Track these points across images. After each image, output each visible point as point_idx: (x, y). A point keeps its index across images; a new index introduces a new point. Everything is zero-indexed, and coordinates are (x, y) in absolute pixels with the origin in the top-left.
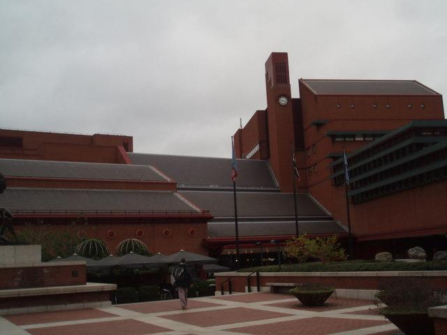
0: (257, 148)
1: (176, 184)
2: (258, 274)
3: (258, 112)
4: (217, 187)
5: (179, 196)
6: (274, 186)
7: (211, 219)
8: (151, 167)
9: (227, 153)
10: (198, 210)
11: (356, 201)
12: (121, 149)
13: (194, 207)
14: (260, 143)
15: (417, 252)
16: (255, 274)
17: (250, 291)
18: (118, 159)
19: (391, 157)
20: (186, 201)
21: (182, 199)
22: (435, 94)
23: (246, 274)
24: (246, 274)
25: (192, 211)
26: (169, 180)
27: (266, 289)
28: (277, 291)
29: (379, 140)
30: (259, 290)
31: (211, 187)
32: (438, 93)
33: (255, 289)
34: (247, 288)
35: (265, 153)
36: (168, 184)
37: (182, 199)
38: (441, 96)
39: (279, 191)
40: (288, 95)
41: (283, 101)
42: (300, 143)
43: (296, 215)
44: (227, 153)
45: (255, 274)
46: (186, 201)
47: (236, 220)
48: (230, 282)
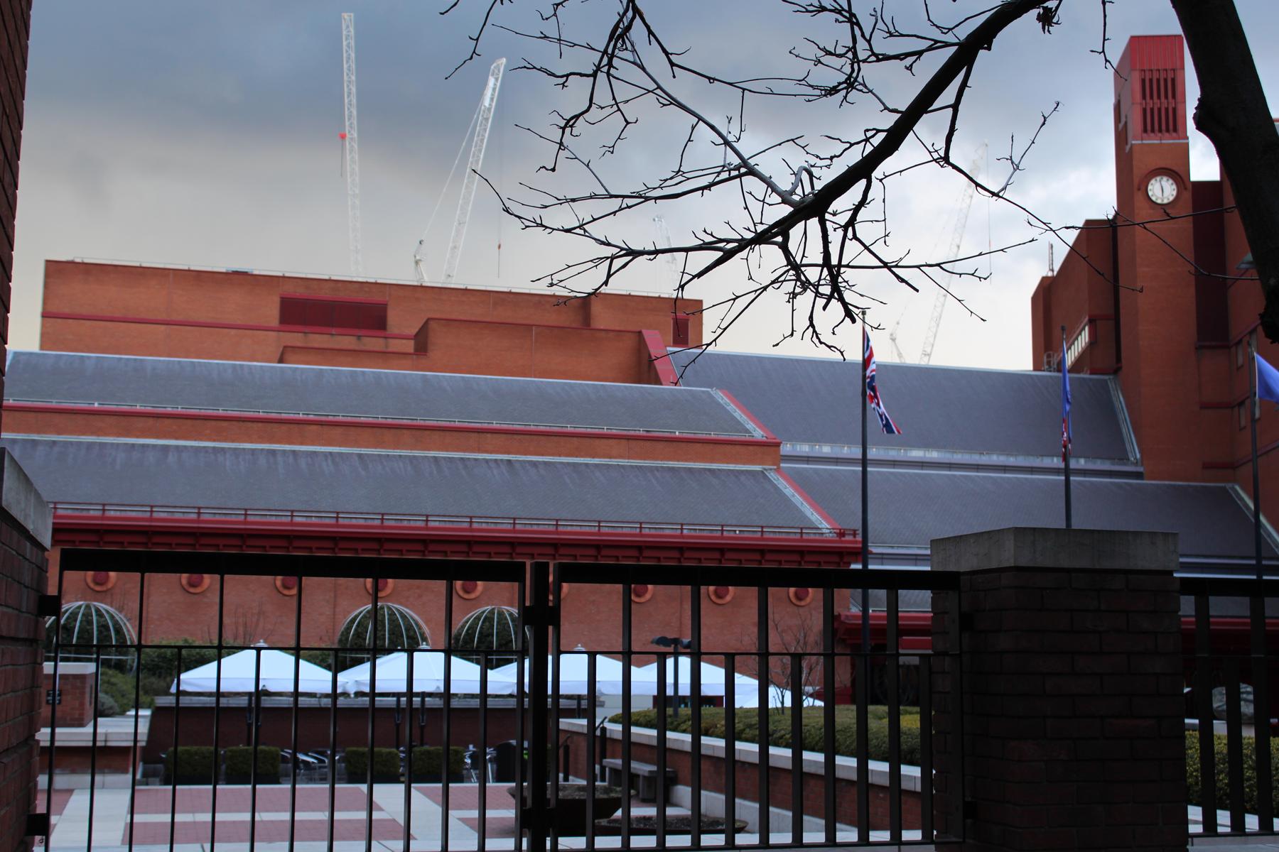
0: (1083, 339)
1: (778, 445)
3: (1091, 228)
4: (934, 455)
6: (1124, 458)
8: (720, 397)
10: (824, 525)
12: (659, 342)
13: (815, 517)
14: (1092, 322)
18: (644, 368)
21: (789, 491)
26: (758, 434)
31: (916, 454)
35: (1108, 356)
37: (789, 491)
39: (1138, 475)
40: (1179, 174)
41: (1162, 190)
46: (797, 499)
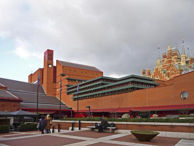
2: (80, 122)
4: (23, 91)
5: (8, 92)
7: (21, 101)
9: (26, 80)
15: (155, 116)
16: (78, 122)
17: (72, 130)
19: (86, 88)
20: (11, 94)
23: (72, 122)
24: (72, 122)
25: (14, 98)
27: (83, 129)
29: (83, 83)
30: (80, 129)
31: (20, 91)
33: (77, 129)
36: (4, 87)
37: (10, 93)
42: (55, 81)
43: (60, 103)
44: (26, 80)
45: (78, 122)
47: (38, 103)
48: (59, 125)
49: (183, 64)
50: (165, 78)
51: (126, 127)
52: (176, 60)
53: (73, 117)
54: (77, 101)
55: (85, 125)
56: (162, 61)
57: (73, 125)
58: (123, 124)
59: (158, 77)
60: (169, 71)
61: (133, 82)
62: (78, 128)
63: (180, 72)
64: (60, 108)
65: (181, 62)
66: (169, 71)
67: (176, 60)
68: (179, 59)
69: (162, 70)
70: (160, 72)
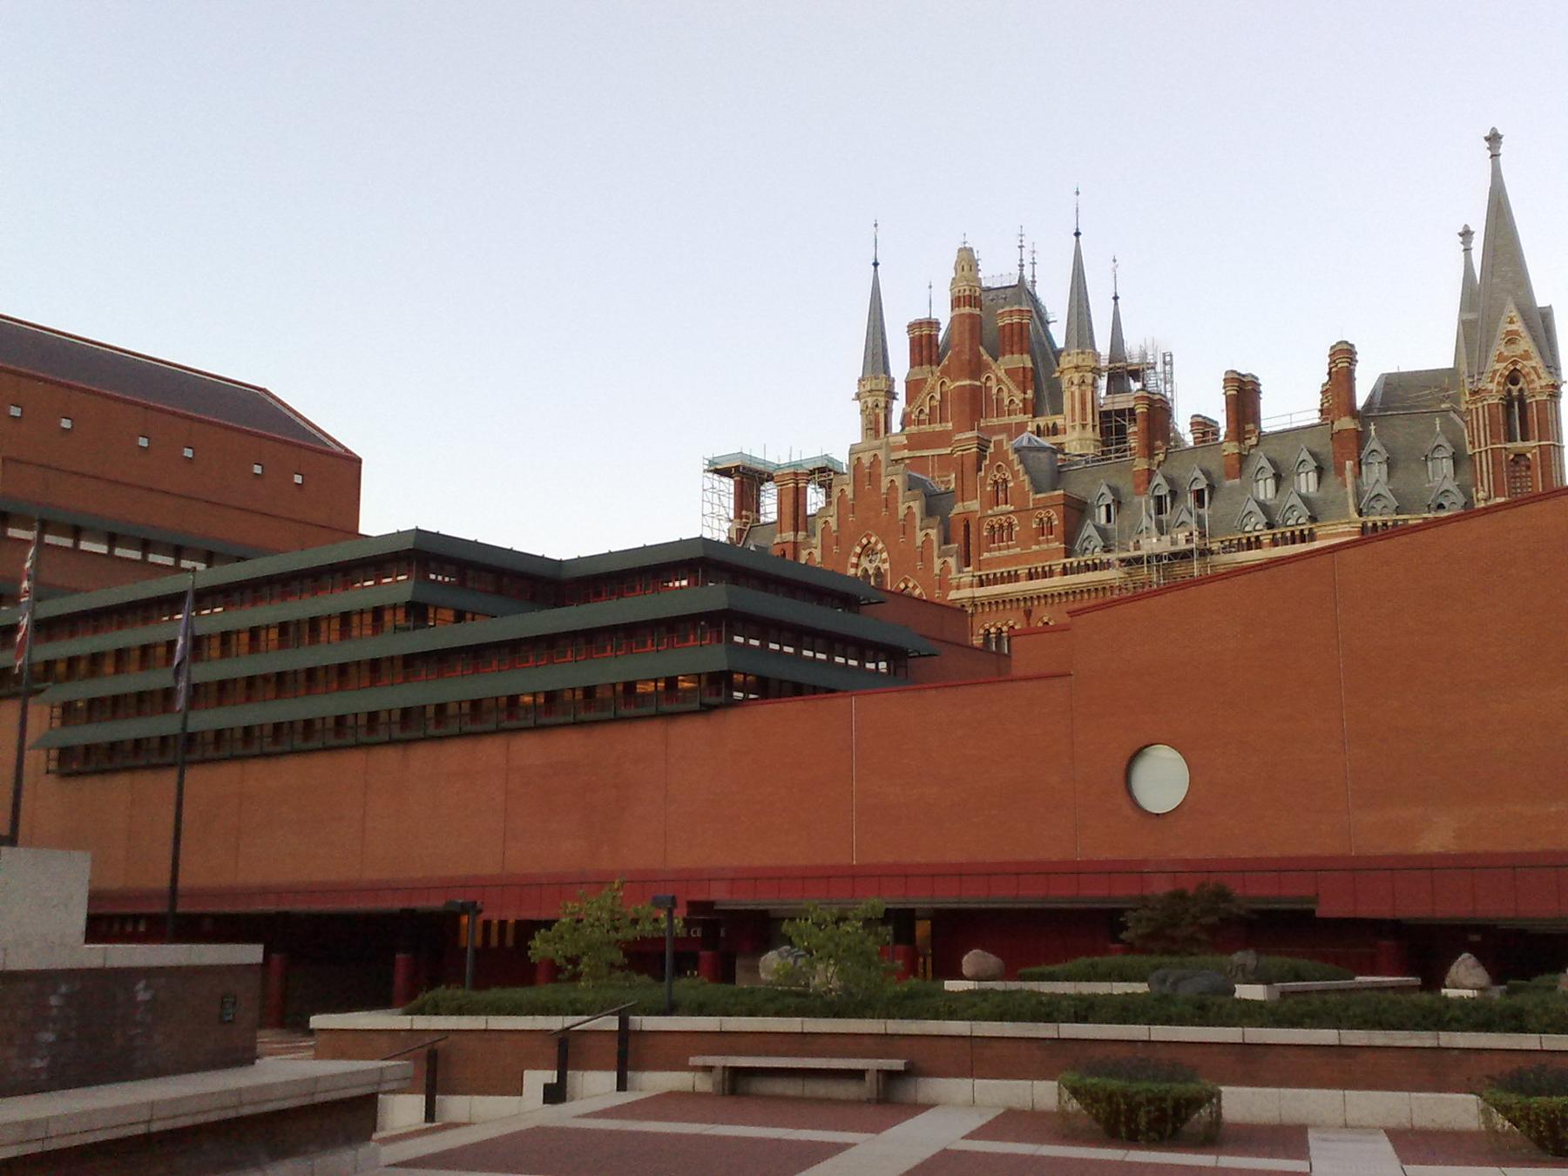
2: (624, 1023)
11: (76, 763)
17: (555, 1094)
22: (338, 449)
23: (556, 1023)
24: (556, 1023)
28: (737, 1082)
30: (622, 1085)
32: (347, 450)
34: (537, 1079)
38: (359, 461)
49: (1078, 440)
50: (937, 564)
51: (976, 1060)
52: (1018, 397)
53: (479, 984)
54: (169, 779)
55: (673, 1052)
56: (900, 389)
57: (567, 1053)
58: (954, 1033)
59: (868, 550)
60: (974, 505)
61: (721, 622)
62: (611, 1077)
63: (1065, 519)
64: (174, 879)
65: (1059, 421)
66: (974, 505)
67: (1018, 397)
68: (1041, 388)
69: (913, 483)
70: (889, 503)
